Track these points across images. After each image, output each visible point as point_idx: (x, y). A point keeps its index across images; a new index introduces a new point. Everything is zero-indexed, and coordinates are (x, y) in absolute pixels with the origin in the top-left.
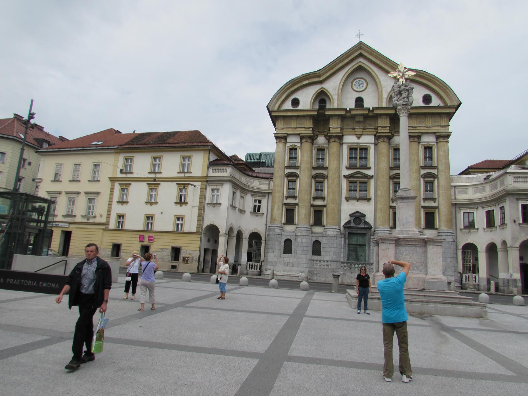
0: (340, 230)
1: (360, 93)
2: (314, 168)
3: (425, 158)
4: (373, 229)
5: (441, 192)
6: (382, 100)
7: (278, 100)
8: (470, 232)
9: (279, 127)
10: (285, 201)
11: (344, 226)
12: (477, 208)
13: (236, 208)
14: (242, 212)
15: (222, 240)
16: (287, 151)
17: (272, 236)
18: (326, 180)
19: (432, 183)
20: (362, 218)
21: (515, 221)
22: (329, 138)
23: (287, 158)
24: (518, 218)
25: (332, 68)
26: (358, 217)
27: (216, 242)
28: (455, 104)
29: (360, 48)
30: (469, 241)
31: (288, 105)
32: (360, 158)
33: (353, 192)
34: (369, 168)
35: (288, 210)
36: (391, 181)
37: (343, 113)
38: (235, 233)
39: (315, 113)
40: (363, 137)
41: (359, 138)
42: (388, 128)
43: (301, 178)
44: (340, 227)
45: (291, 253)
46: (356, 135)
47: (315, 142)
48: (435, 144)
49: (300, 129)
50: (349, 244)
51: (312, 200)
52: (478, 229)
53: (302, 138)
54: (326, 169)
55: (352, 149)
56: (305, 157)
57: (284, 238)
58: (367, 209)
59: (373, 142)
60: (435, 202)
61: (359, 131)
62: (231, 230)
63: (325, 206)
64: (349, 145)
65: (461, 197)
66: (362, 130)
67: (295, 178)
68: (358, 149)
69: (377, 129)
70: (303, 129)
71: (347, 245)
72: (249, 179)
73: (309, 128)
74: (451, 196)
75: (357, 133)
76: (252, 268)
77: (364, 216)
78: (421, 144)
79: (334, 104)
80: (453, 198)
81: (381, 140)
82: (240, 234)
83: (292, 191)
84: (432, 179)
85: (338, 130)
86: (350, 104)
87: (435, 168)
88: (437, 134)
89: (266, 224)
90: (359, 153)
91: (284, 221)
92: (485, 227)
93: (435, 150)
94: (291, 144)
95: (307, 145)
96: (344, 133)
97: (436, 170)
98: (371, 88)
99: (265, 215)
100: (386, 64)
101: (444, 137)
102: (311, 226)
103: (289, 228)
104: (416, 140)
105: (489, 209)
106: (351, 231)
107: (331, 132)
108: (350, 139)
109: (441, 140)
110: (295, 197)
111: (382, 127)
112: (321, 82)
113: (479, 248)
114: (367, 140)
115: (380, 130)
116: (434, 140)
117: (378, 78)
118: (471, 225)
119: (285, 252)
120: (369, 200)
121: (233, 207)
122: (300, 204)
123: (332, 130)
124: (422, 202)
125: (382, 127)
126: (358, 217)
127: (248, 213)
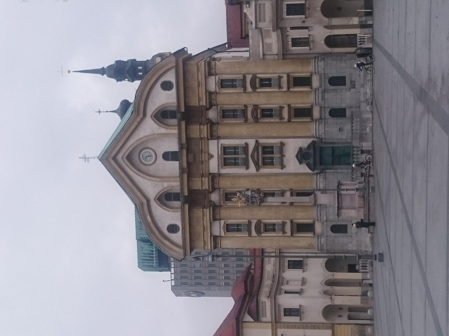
0: (317, 174)
3: (234, 86)
4: (315, 139)
9: (203, 246)
13: (301, 289)
14: (304, 282)
15: (338, 301)
16: (230, 234)
17: (329, 247)
19: (262, 80)
23: (238, 234)
25: (131, 190)
26: (302, 156)
27: (340, 308)
29: (107, 159)
31: (177, 237)
34: (247, 144)
36: (260, 121)
37: (185, 176)
38: (328, 288)
39: (187, 206)
40: (211, 152)
41: (212, 156)
42: (202, 126)
43: (261, 218)
44: (315, 174)
45: (346, 226)
46: (209, 159)
47: (217, 204)
48: (217, 77)
49: (205, 221)
53: (215, 219)
55: (226, 163)
57: (330, 233)
58: (293, 146)
59: (216, 141)
61: (205, 157)
62: (326, 293)
64: (220, 166)
65: (275, 48)
66: (203, 154)
67: (262, 225)
68: (225, 156)
69: (201, 139)
70: (205, 218)
71: (334, 167)
72: (266, 275)
74: (274, 60)
75: (207, 159)
76: (366, 267)
77: (301, 149)
78: (218, 91)
79: (175, 186)
80: (276, 57)
82: (331, 283)
83: (276, 227)
84: (257, 80)
86: (173, 167)
87: (244, 77)
90: (230, 156)
91: (311, 235)
93: (225, 77)
94: (222, 230)
95: (224, 213)
97: (247, 76)
100: (127, 131)
103: (318, 228)
104: (213, 96)
106: (319, 162)
107: (207, 188)
108: (214, 166)
109: (213, 71)
110: (284, 224)
112: (148, 201)
114: (214, 147)
115: (205, 134)
116: (213, 77)
117: (142, 138)
119: (346, 232)
120: (282, 144)
121: (300, 293)
122: (291, 217)
123: (206, 186)
124: (282, 90)
126: (302, 156)
127: (305, 275)
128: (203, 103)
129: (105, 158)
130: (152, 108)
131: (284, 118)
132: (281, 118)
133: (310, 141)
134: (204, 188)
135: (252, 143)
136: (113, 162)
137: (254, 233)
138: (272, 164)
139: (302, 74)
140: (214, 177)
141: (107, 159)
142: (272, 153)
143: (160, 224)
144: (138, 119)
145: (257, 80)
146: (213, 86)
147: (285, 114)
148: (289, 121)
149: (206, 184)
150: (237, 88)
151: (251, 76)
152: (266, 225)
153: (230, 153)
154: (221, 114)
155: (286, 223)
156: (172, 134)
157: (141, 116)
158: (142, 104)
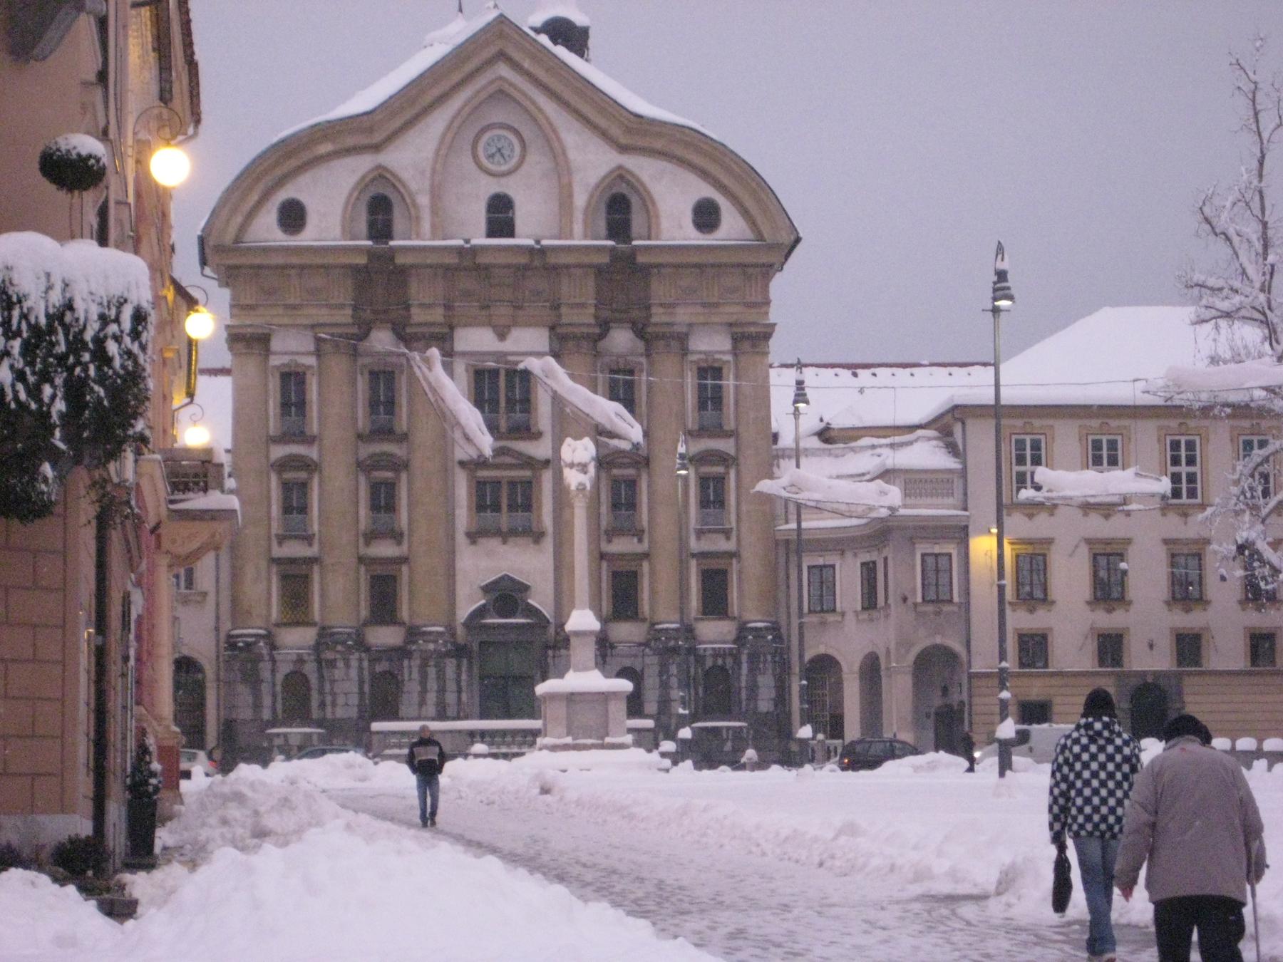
1: (504, 180)
2: (360, 437)
4: (552, 630)
5: (744, 508)
6: (571, 215)
7: (234, 210)
8: (823, 624)
10: (278, 552)
11: (466, 625)
12: (843, 553)
16: (274, 384)
18: (404, 476)
19: (720, 480)
20: (518, 596)
21: (905, 599)
22: (405, 337)
24: (914, 590)
28: (787, 239)
29: (501, 35)
30: (822, 650)
31: (267, 229)
32: (510, 401)
33: (489, 514)
34: (538, 435)
35: (284, 578)
41: (502, 336)
42: (592, 310)
47: (363, 346)
48: (729, 358)
50: (482, 678)
51: (361, 541)
52: (843, 614)
54: (404, 438)
56: (336, 405)
60: (728, 538)
63: (404, 560)
67: (303, 475)
68: (502, 374)
69: (556, 307)
70: (324, 311)
71: (476, 681)
73: (342, 306)
77: (526, 588)
81: (571, 344)
84: (720, 469)
85: (438, 315)
87: (728, 435)
88: (735, 330)
89: (217, 629)
92: (859, 608)
94: (286, 359)
95: (338, 366)
96: (455, 321)
97: (732, 441)
98: (537, 162)
99: (211, 599)
101: (752, 339)
102: (365, 624)
104: (674, 344)
105: (867, 557)
108: (476, 339)
109: (746, 346)
110: (308, 539)
111: (572, 306)
112: (376, 148)
113: (845, 668)
115: (568, 316)
117: (558, 138)
118: (824, 602)
120: (538, 537)
122: (328, 560)
123: (418, 315)
125: (572, 306)
128: (658, 316)
129: (507, 29)
130: (645, 169)
131: (610, 541)
132: (612, 534)
133: (548, 613)
134: (414, 311)
135: (540, 449)
136: (492, 50)
137: (278, 452)
138: (480, 507)
139: (735, 595)
140: (444, 340)
141: (501, 35)
142: (512, 507)
143: (304, 180)
144: (615, 131)
145: (720, 469)
146: (703, 347)
147: (621, 545)
148: (602, 556)
149: (424, 316)
150: (696, 414)
151: (732, 452)
152: (304, 486)
153: (510, 387)
154: (622, 366)
155: (310, 545)
156: (572, 222)
157: (623, 140)
158: (659, 144)
